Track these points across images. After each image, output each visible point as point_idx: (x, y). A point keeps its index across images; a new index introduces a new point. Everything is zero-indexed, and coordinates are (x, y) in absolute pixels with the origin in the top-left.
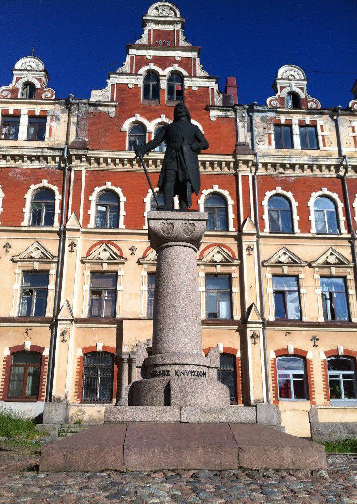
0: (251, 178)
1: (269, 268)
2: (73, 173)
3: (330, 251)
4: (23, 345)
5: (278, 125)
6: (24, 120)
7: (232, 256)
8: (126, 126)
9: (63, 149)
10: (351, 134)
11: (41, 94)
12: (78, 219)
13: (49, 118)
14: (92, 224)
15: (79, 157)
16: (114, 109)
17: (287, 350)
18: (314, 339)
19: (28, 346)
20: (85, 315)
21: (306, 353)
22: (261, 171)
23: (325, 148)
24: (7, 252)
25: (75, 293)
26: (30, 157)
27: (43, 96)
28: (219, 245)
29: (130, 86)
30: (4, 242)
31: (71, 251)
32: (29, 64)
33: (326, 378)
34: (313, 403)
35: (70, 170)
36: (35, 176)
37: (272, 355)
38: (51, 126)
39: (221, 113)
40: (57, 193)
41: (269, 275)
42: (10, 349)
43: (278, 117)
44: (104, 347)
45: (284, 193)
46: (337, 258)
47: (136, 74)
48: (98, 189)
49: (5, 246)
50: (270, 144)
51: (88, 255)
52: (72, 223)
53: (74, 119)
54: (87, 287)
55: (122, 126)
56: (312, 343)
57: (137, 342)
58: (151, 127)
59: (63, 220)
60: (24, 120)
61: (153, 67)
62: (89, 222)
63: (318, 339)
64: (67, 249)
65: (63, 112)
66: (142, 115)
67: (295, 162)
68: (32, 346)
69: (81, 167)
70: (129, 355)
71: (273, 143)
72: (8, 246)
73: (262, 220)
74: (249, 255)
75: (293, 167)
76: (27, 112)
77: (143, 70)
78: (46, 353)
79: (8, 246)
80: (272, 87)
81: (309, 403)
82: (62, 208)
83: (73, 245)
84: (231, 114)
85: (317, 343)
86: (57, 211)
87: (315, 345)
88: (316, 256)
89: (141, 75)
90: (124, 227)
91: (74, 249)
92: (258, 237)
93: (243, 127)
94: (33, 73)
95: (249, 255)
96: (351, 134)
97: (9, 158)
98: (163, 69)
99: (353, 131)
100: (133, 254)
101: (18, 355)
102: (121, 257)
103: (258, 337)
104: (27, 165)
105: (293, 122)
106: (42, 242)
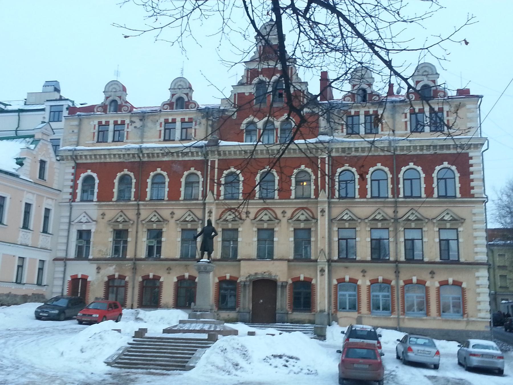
1: (336, 224)
2: (209, 162)
3: (377, 212)
4: (184, 276)
7: (311, 215)
8: (243, 126)
10: (404, 120)
11: (188, 105)
12: (213, 194)
13: (194, 123)
15: (213, 152)
17: (344, 279)
18: (364, 271)
19: (187, 275)
21: (357, 281)
22: (334, 154)
23: (383, 133)
24: (172, 217)
27: (190, 107)
28: (303, 209)
29: (247, 94)
30: (170, 211)
32: (179, 83)
34: (360, 313)
35: (208, 160)
36: (186, 165)
37: (335, 282)
38: (195, 129)
40: (200, 176)
41: (336, 229)
42: (177, 277)
44: (230, 276)
45: (350, 168)
46: (383, 216)
47: (251, 84)
49: (171, 214)
51: (220, 219)
52: (210, 198)
53: (210, 123)
56: (362, 274)
59: (205, 196)
60: (178, 125)
61: (261, 77)
63: (365, 272)
65: (203, 117)
68: (189, 276)
69: (214, 158)
71: (345, 130)
72: (172, 213)
74: (323, 215)
75: (357, 149)
76: (180, 120)
77: (256, 81)
79: (172, 213)
81: (356, 313)
82: (203, 187)
83: (210, 212)
85: (365, 274)
87: (364, 276)
88: (369, 214)
91: (211, 215)
92: (329, 203)
93: (323, 120)
94: (182, 90)
95: (323, 215)
96: (404, 120)
100: (247, 217)
101: (181, 279)
103: (324, 271)
105: (360, 113)
106: (192, 210)
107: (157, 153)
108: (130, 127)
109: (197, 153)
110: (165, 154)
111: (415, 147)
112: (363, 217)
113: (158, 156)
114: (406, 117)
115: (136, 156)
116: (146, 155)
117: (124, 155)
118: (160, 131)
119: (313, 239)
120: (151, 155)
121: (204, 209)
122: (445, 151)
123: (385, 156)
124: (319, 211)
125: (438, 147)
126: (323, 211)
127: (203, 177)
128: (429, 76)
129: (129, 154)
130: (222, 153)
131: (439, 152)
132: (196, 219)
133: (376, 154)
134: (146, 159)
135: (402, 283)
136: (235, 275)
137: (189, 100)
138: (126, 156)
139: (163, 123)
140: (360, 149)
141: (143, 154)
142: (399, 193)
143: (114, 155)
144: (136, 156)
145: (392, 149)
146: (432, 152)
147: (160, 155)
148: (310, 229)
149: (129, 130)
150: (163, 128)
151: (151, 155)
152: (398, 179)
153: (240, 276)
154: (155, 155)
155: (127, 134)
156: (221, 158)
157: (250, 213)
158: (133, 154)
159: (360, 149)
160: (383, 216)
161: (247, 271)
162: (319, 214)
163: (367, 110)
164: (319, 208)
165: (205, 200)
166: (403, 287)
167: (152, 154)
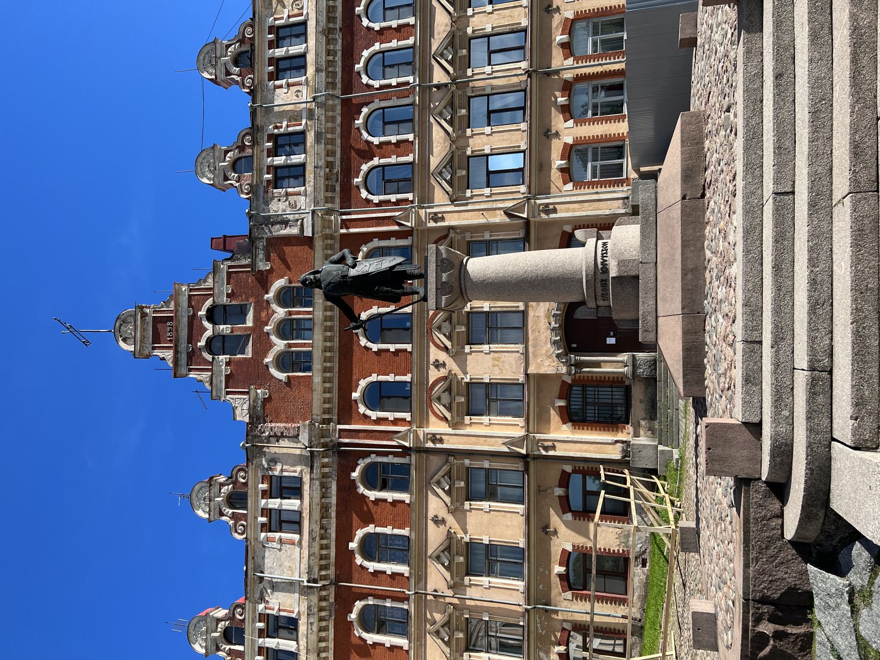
0: (344, 217)
4: (559, 497)
5: (276, 183)
6: (274, 503)
9: (312, 452)
14: (407, 416)
16: (259, 391)
19: (559, 491)
20: (521, 421)
22: (337, 206)
25: (494, 432)
26: (324, 496)
27: (243, 481)
31: (441, 441)
33: (598, 120)
36: (347, 488)
37: (570, 186)
39: (261, 256)
40: (368, 460)
43: (265, 184)
44: (560, 397)
46: (445, 108)
47: (211, 363)
48: (362, 409)
50: (299, 194)
54: (485, 419)
55: (281, 381)
57: (554, 355)
58: (279, 344)
60: (274, 503)
61: (202, 343)
62: (404, 420)
64: (439, 446)
66: (266, 357)
67: (323, 161)
68: (560, 486)
69: (335, 430)
70: (572, 365)
73: (398, 202)
75: (330, 165)
78: (568, 468)
80: (224, 191)
82: (386, 454)
83: (434, 438)
84: (261, 244)
86: (390, 459)
89: (213, 358)
90: (409, 375)
97: (324, 521)
98: (206, 330)
99: (281, 87)
102: (445, 378)
104: (334, 500)
107: (322, 547)
108: (271, 605)
109: (324, 466)
110: (323, 532)
111: (329, 63)
112: (448, 144)
113: (327, 547)
114: (281, 87)
115: (324, 593)
116: (323, 573)
117: (321, 619)
118: (281, 541)
119: (487, 236)
120: (323, 562)
121: (429, 451)
122: (339, 14)
123: (342, 115)
124: (432, 224)
125: (331, 25)
126: (436, 218)
127: (367, 454)
128: (218, 55)
129: (321, 609)
130: (327, 416)
131: (339, 24)
132: (446, 468)
133: (338, 130)
134: (331, 572)
135: (570, 62)
136: (556, 389)
137: (233, 483)
138: (323, 614)
139: (270, 534)
140: (330, 159)
141: (323, 578)
142: (408, 83)
143: (321, 640)
144: (324, 593)
145: (331, 102)
146: (338, 36)
147: (325, 542)
148: (469, 243)
149: (277, 608)
150: (277, 535)
151: (323, 562)
152: (382, 87)
153: (558, 376)
154: (324, 552)
155: (284, 610)
156: (335, 417)
157: (437, 361)
158: (322, 599)
159: (330, 159)
160: (445, 108)
161: (547, 360)
162: (439, 224)
163: (265, 153)
164: (429, 225)
165: (410, 449)
166: (577, 60)
167: (321, 559)
